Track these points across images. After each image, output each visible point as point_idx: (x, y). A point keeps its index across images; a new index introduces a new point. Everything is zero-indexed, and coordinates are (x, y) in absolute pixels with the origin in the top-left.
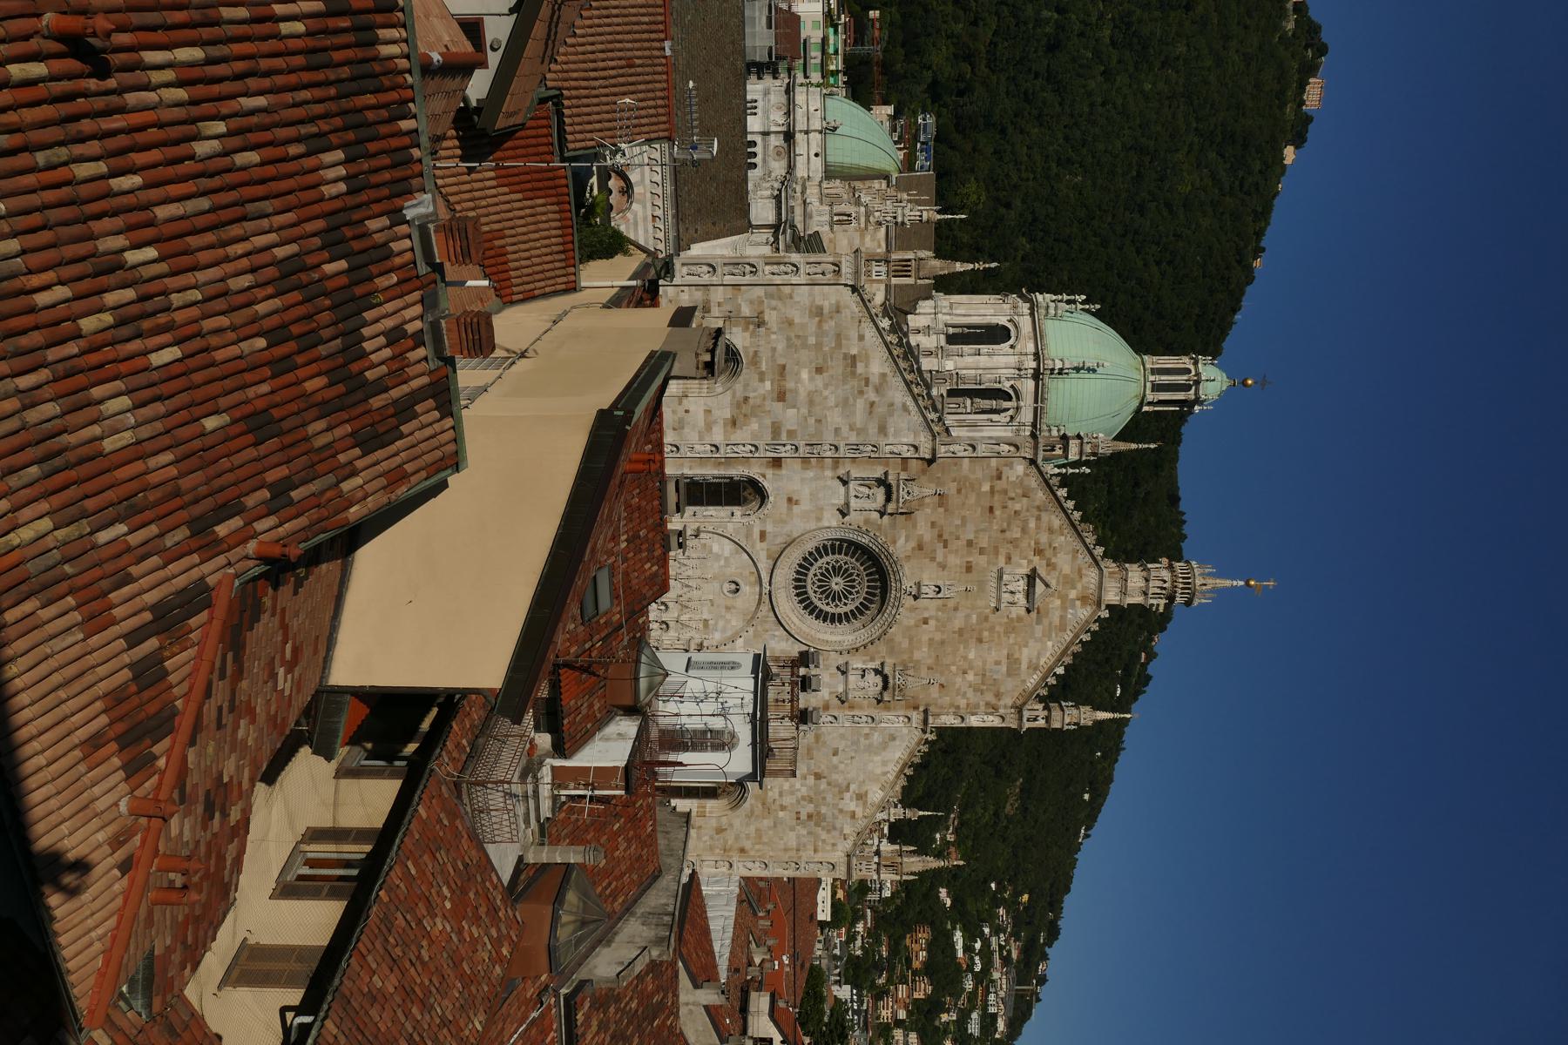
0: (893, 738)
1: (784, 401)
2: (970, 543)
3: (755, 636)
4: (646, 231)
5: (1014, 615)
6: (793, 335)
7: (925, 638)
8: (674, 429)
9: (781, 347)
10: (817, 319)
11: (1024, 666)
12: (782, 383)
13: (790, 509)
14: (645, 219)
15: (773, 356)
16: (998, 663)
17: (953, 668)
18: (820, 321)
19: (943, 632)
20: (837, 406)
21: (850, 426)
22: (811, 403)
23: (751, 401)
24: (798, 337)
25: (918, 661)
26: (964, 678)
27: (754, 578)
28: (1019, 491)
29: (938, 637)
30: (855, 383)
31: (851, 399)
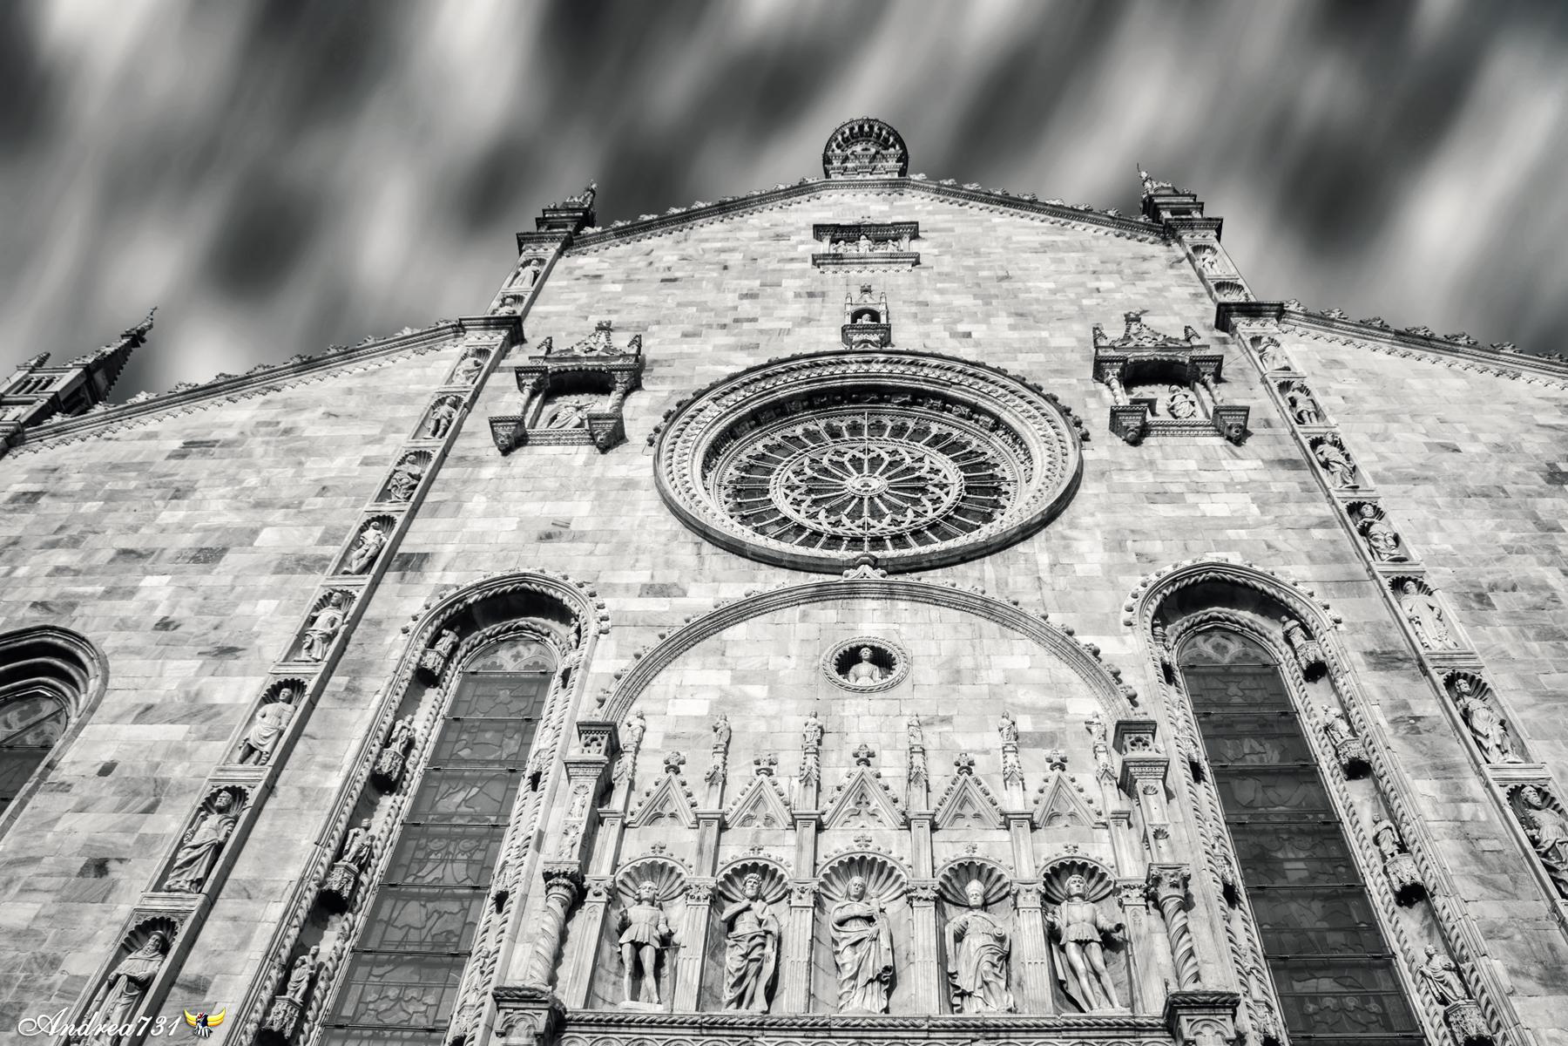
1: (225, 550)
2: (750, 296)
3: (1061, 609)
5: (936, 251)
7: (1015, 335)
8: (150, 809)
9: (62, 557)
11: (1058, 238)
13: (579, 537)
16: (1062, 261)
17: (1085, 302)
19: (988, 316)
20: (300, 463)
21: (370, 442)
22: (259, 505)
24: (62, 528)
25: (1079, 340)
26: (1110, 291)
27: (827, 613)
29: (1003, 320)
31: (298, 444)
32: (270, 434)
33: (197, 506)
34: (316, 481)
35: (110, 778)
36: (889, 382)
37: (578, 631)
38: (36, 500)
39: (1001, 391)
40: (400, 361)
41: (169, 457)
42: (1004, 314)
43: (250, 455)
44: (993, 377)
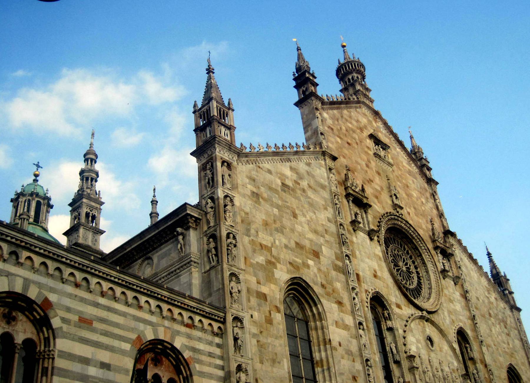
0: (461, 259)
4: (200, 339)
6: (274, 225)
7: (415, 218)
8: (354, 361)
10: (261, 200)
12: (307, 248)
13: (380, 279)
14: (189, 337)
15: (291, 251)
17: (423, 208)
18: (262, 198)
22: (316, 232)
23: (324, 282)
24: (275, 221)
28: (336, 122)
30: (299, 192)
32: (300, 189)
33: (301, 224)
34: (323, 224)
35: (342, 348)
36: (404, 231)
37: (389, 314)
38: (259, 198)
39: (423, 248)
40: (313, 160)
41: (282, 190)
42: (412, 206)
43: (301, 201)
44: (423, 242)
